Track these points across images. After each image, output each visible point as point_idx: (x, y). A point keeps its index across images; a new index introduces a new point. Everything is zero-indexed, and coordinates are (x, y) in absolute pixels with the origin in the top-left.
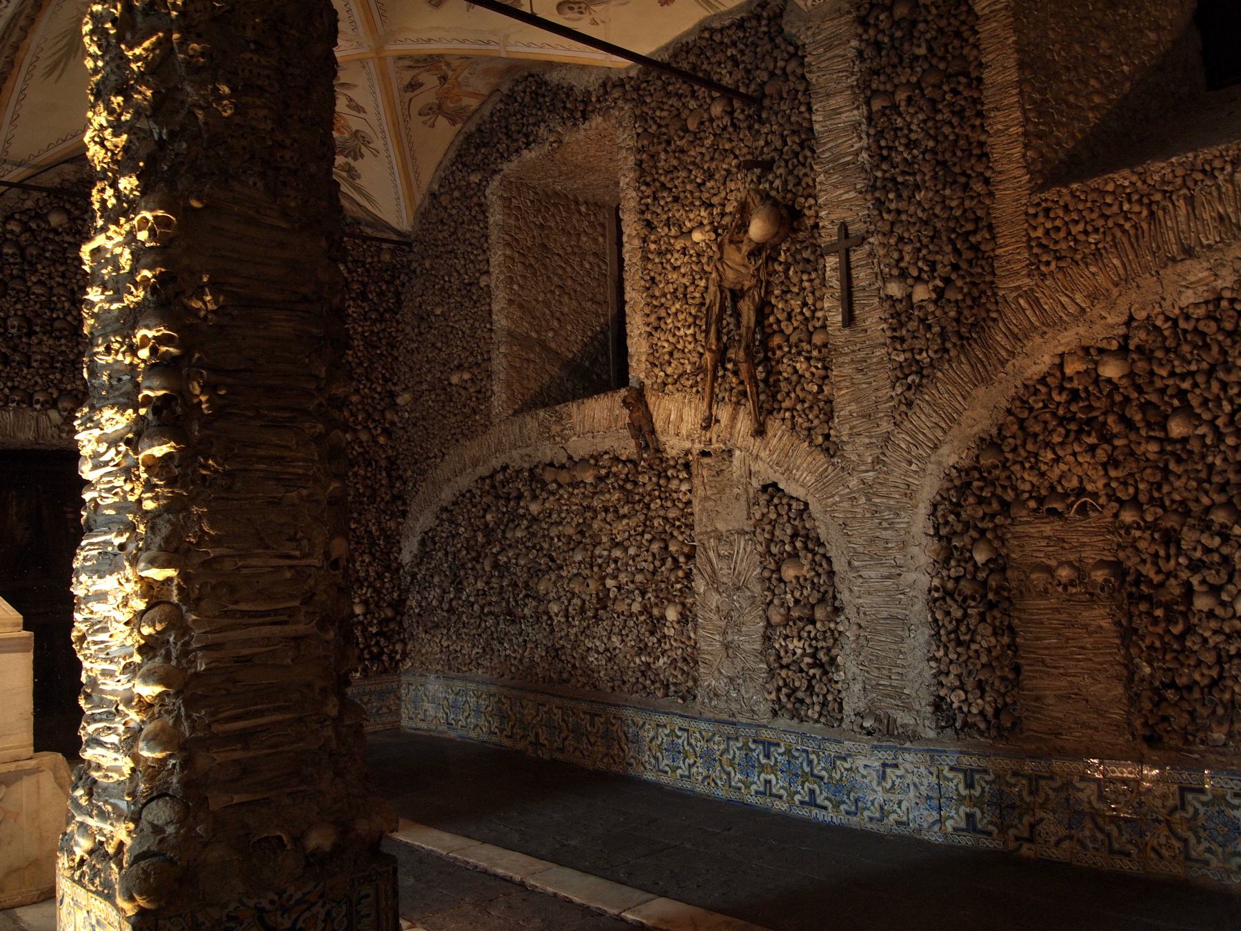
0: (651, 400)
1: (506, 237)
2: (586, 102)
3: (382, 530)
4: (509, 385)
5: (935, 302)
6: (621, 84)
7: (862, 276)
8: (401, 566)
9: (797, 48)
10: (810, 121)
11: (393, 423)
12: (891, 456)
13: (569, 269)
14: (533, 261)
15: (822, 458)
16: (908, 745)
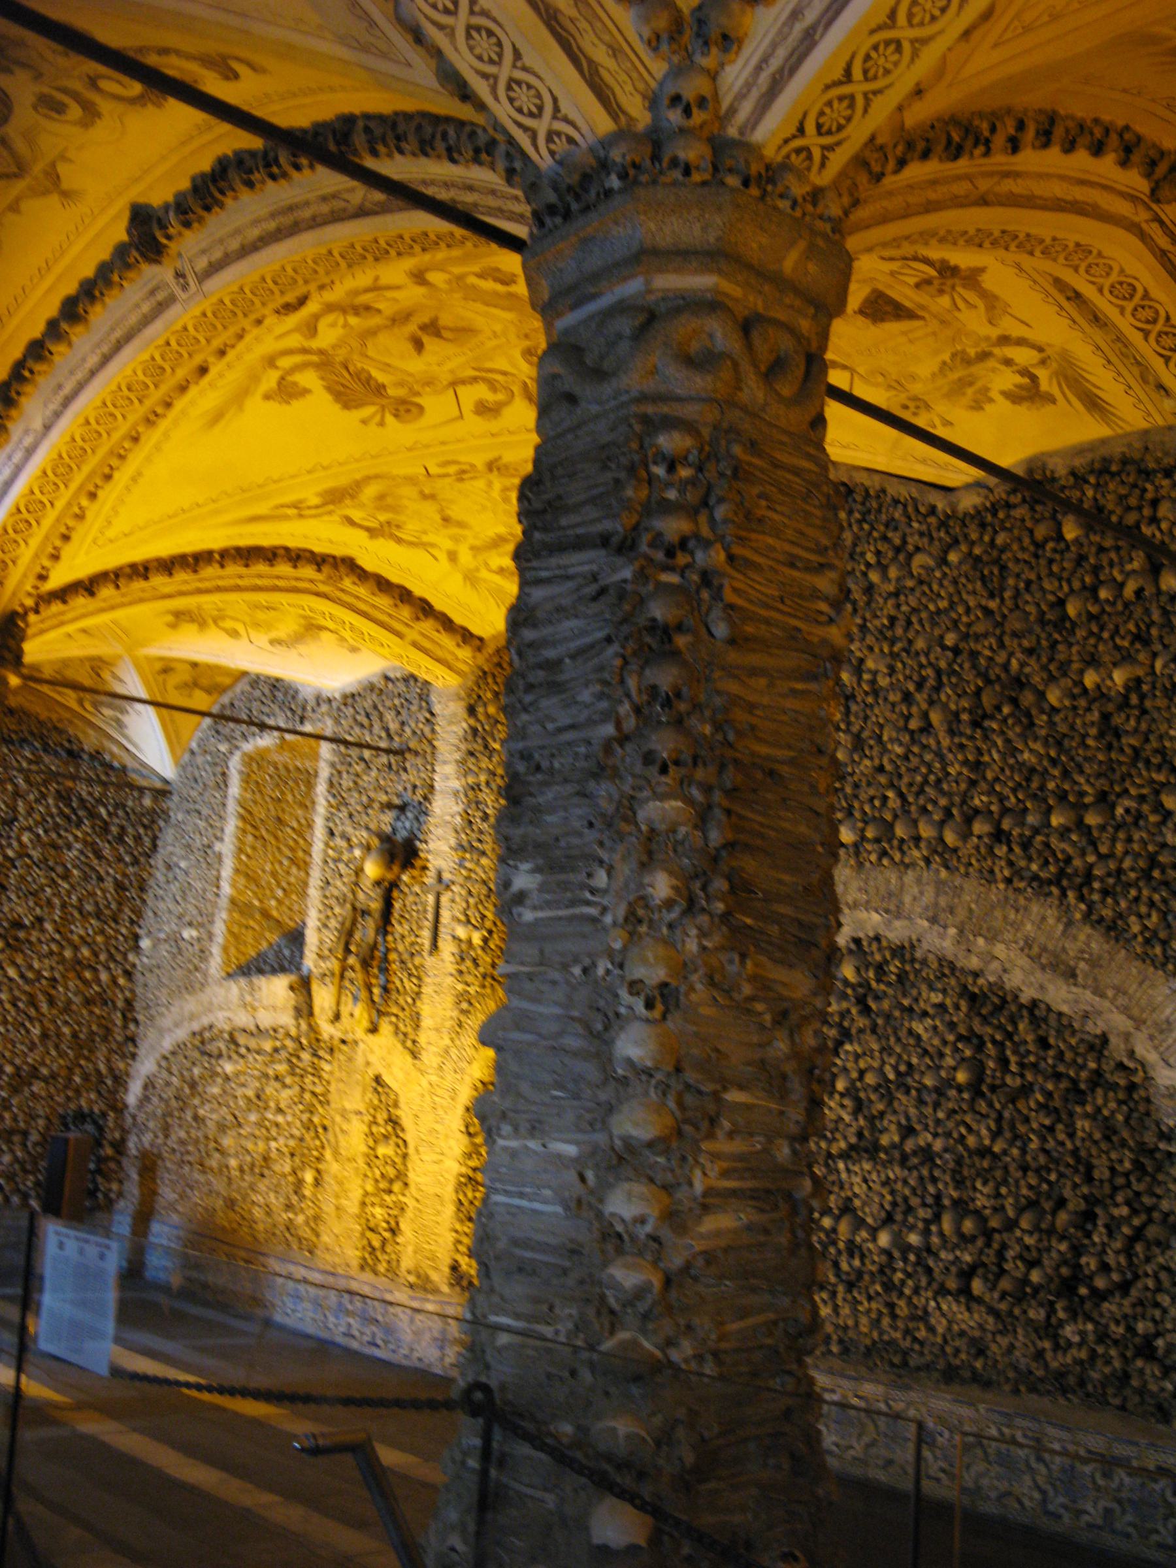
0: (315, 987)
1: (241, 811)
2: (304, 709)
3: (111, 1070)
4: (225, 949)
5: (483, 949)
6: (329, 701)
7: (445, 916)
8: (126, 1106)
9: (432, 714)
10: (432, 779)
11: (134, 966)
12: (449, 1066)
13: (301, 842)
14: (264, 833)
15: (409, 1058)
16: (430, 1297)
